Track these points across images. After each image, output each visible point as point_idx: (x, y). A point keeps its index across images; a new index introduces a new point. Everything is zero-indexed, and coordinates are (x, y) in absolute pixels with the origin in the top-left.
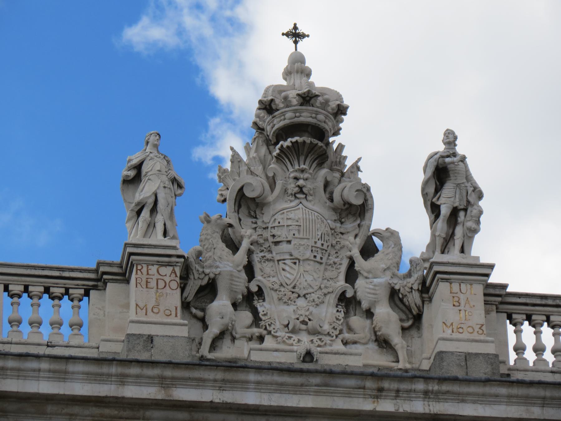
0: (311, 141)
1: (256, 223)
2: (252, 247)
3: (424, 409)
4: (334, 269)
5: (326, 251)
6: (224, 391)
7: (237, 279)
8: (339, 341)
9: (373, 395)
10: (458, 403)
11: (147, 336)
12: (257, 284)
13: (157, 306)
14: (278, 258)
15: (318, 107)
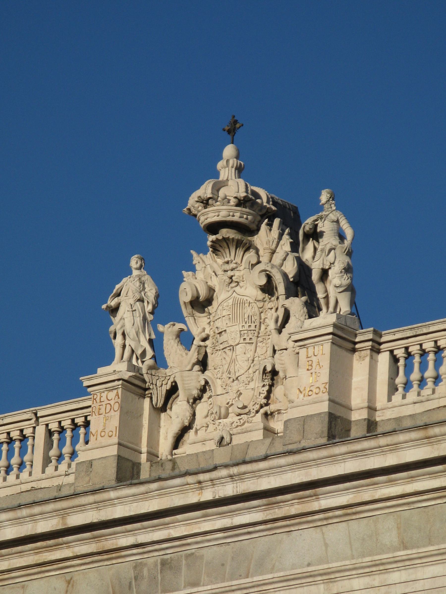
0: (223, 237)
1: (209, 318)
2: (202, 344)
3: (233, 491)
4: (264, 344)
5: (255, 330)
6: (101, 511)
7: (187, 379)
8: (259, 415)
9: (198, 488)
10: (257, 479)
11: (88, 462)
12: (203, 378)
13: (103, 430)
14: (222, 347)
15: (218, 205)
